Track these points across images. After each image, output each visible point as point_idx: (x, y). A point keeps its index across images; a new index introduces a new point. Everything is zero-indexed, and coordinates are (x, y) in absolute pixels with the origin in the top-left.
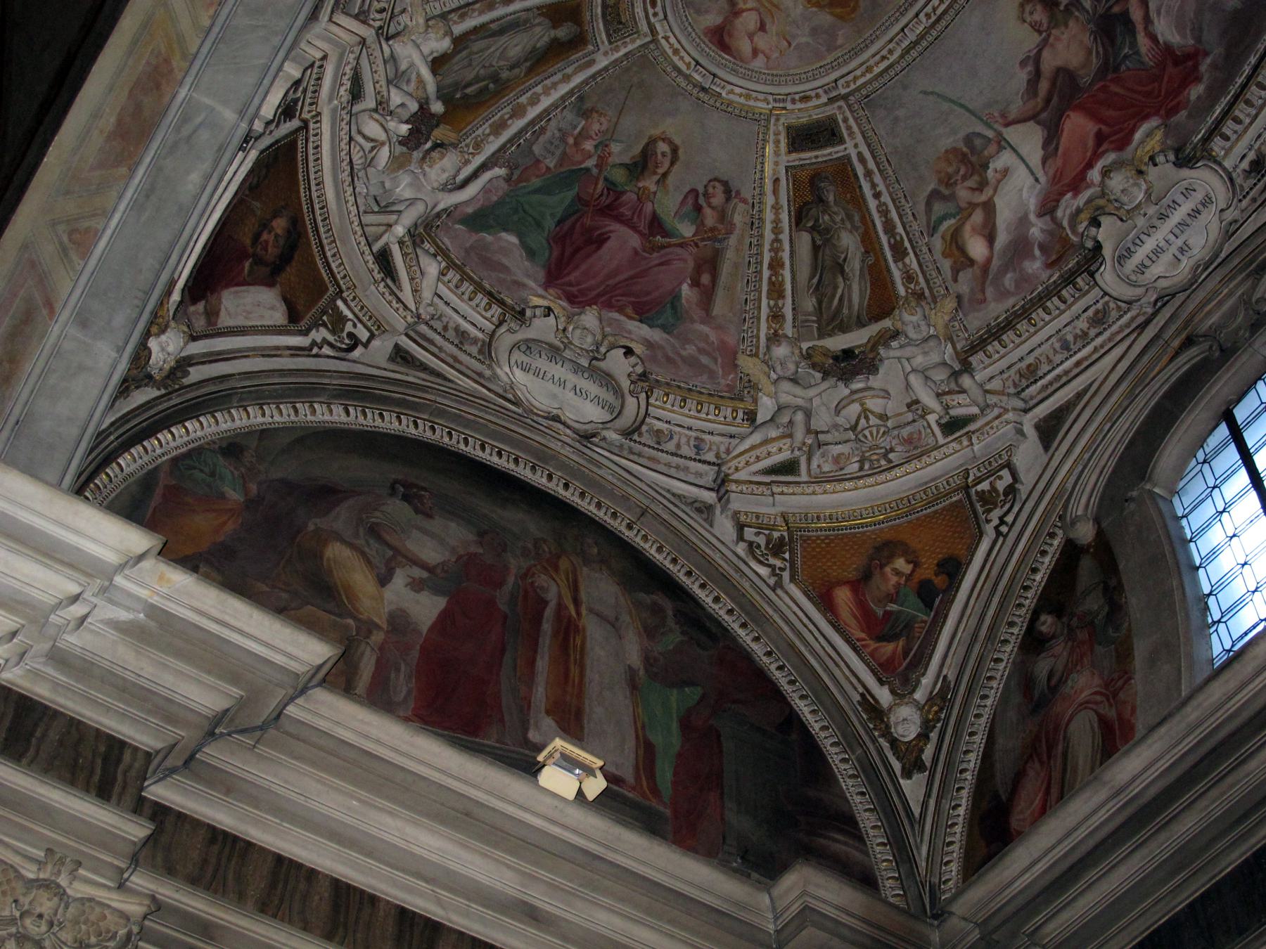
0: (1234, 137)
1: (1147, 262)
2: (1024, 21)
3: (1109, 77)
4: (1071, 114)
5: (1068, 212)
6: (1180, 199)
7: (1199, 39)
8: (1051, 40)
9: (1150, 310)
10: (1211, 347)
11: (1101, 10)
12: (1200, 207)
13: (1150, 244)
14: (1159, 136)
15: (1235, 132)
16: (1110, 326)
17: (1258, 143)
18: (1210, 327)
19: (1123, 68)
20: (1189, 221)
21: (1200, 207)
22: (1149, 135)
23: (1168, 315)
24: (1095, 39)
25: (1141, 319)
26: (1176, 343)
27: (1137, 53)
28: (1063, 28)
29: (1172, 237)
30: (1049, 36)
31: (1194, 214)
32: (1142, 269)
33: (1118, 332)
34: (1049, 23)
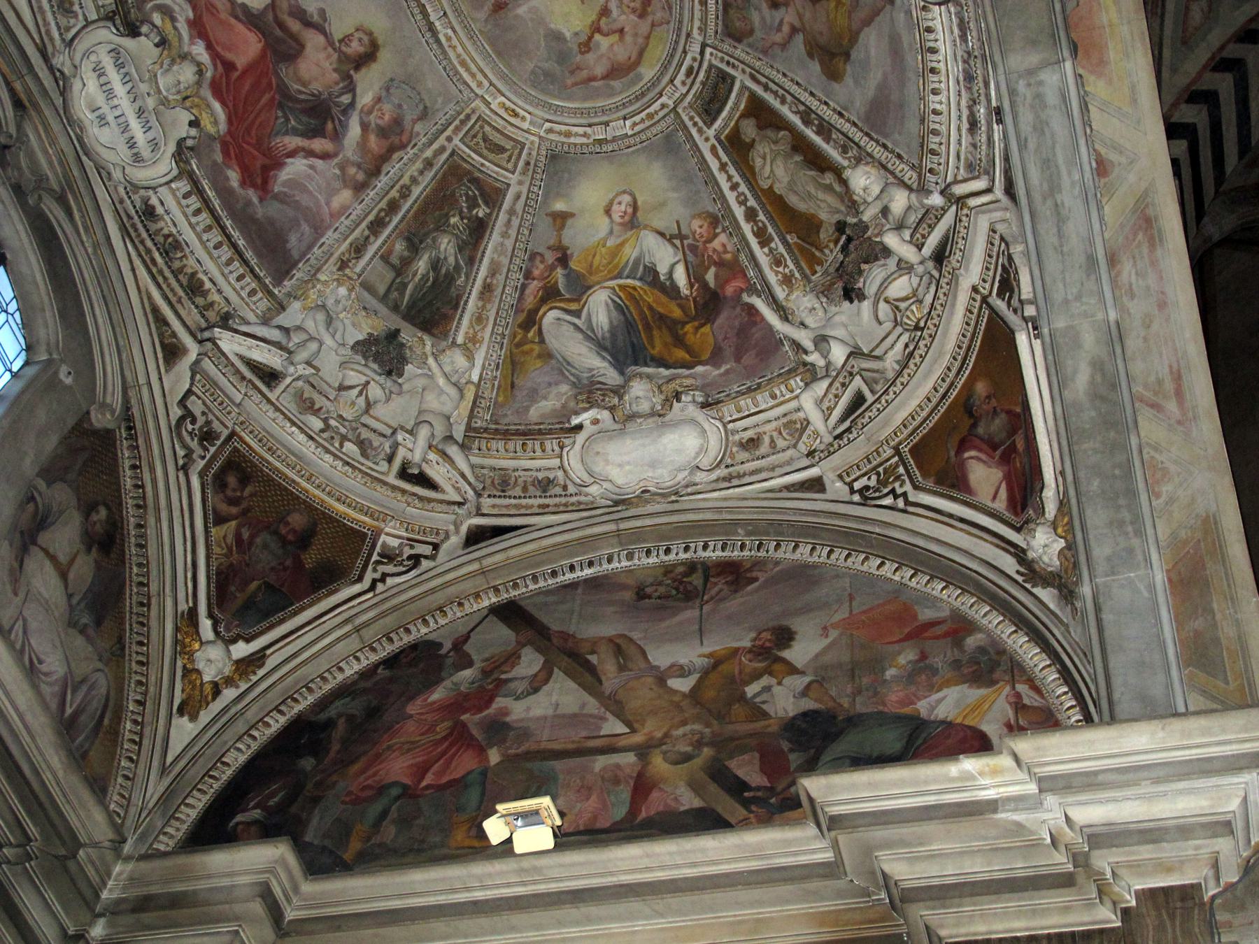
0: (184, 202)
1: (103, 79)
2: (357, 30)
3: (277, 97)
4: (260, 46)
5: (176, 8)
6: (150, 135)
7: (276, 197)
8: (330, 49)
9: (54, 62)
10: (11, 137)
11: (335, 110)
12: (135, 151)
13: (120, 89)
14: (210, 129)
15: (188, 206)
16: (54, 13)
17: (169, 220)
18: (27, 136)
19: (280, 114)
20: (126, 135)
21: (135, 151)
22: (216, 123)
23: (46, 83)
24: (313, 95)
25: (50, 49)
26: (18, 86)
27: (286, 133)
28: (335, 66)
29: (118, 113)
30: (334, 49)
31: (131, 143)
32: (99, 71)
33: (44, 20)
34: (344, 53)
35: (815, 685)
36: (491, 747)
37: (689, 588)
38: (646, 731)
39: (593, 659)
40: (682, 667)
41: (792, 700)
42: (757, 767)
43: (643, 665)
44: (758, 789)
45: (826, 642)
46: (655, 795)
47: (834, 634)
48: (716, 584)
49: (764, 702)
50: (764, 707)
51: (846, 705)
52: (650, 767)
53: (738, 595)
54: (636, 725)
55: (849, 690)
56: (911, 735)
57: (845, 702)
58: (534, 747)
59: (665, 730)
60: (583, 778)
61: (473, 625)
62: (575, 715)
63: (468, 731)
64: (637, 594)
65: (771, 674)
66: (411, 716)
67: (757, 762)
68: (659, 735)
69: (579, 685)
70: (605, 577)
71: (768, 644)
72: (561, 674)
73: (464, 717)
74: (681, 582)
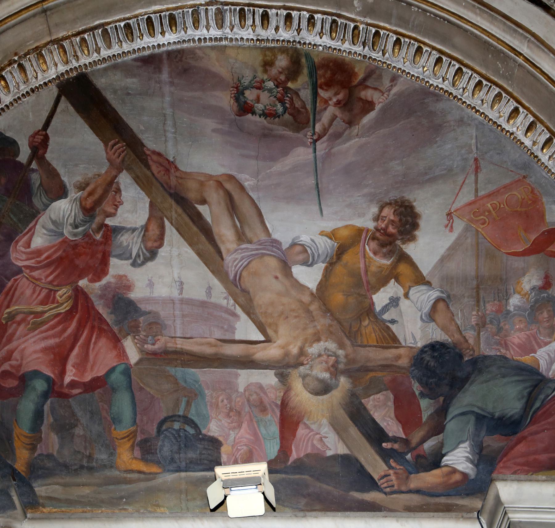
35: (441, 305)
36: (125, 337)
37: (298, 104)
38: (280, 342)
39: (203, 209)
40: (304, 249)
41: (420, 323)
42: (393, 415)
43: (263, 237)
44: (395, 440)
45: (453, 237)
46: (301, 431)
47: (459, 225)
48: (326, 102)
49: (393, 322)
50: (394, 328)
51: (471, 341)
52: (293, 393)
53: (355, 130)
54: (270, 332)
55: (474, 321)
56: (530, 394)
57: (470, 335)
58: (171, 345)
59: (299, 344)
60: (229, 399)
61: (45, 115)
62: (203, 304)
63: (93, 308)
64: (237, 99)
65: (397, 280)
66: (19, 271)
67: (391, 404)
68: (295, 350)
69: (199, 254)
70: (191, 51)
71: (391, 229)
72: (175, 231)
73: (83, 283)
74: (287, 90)
